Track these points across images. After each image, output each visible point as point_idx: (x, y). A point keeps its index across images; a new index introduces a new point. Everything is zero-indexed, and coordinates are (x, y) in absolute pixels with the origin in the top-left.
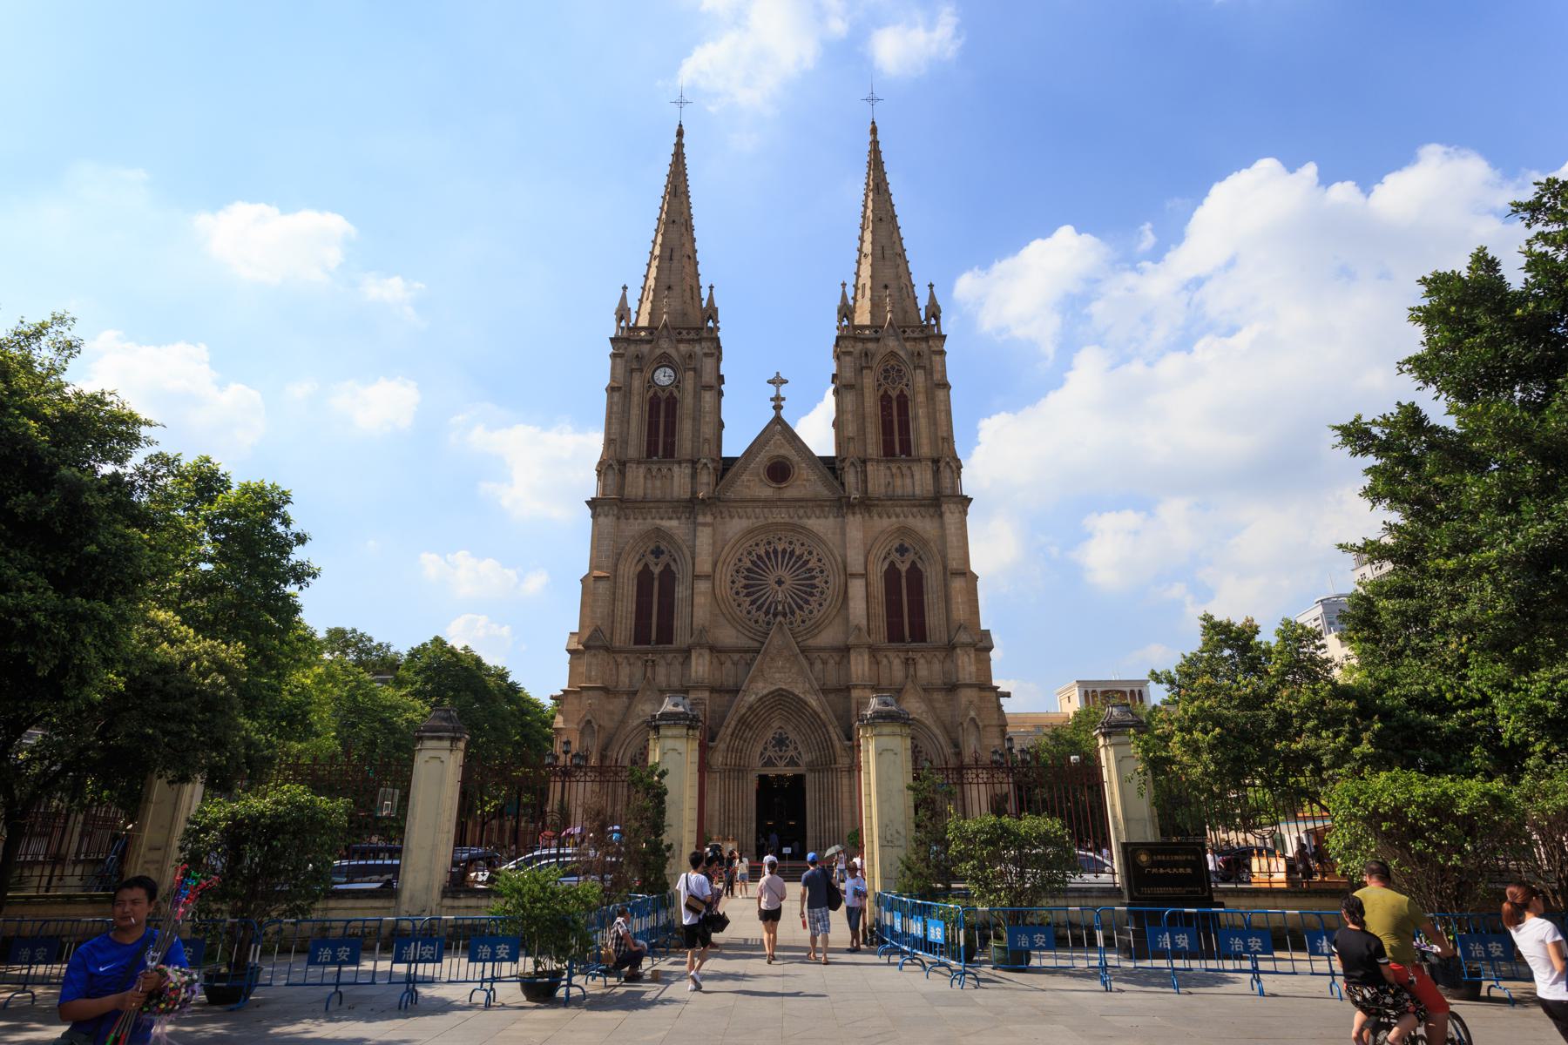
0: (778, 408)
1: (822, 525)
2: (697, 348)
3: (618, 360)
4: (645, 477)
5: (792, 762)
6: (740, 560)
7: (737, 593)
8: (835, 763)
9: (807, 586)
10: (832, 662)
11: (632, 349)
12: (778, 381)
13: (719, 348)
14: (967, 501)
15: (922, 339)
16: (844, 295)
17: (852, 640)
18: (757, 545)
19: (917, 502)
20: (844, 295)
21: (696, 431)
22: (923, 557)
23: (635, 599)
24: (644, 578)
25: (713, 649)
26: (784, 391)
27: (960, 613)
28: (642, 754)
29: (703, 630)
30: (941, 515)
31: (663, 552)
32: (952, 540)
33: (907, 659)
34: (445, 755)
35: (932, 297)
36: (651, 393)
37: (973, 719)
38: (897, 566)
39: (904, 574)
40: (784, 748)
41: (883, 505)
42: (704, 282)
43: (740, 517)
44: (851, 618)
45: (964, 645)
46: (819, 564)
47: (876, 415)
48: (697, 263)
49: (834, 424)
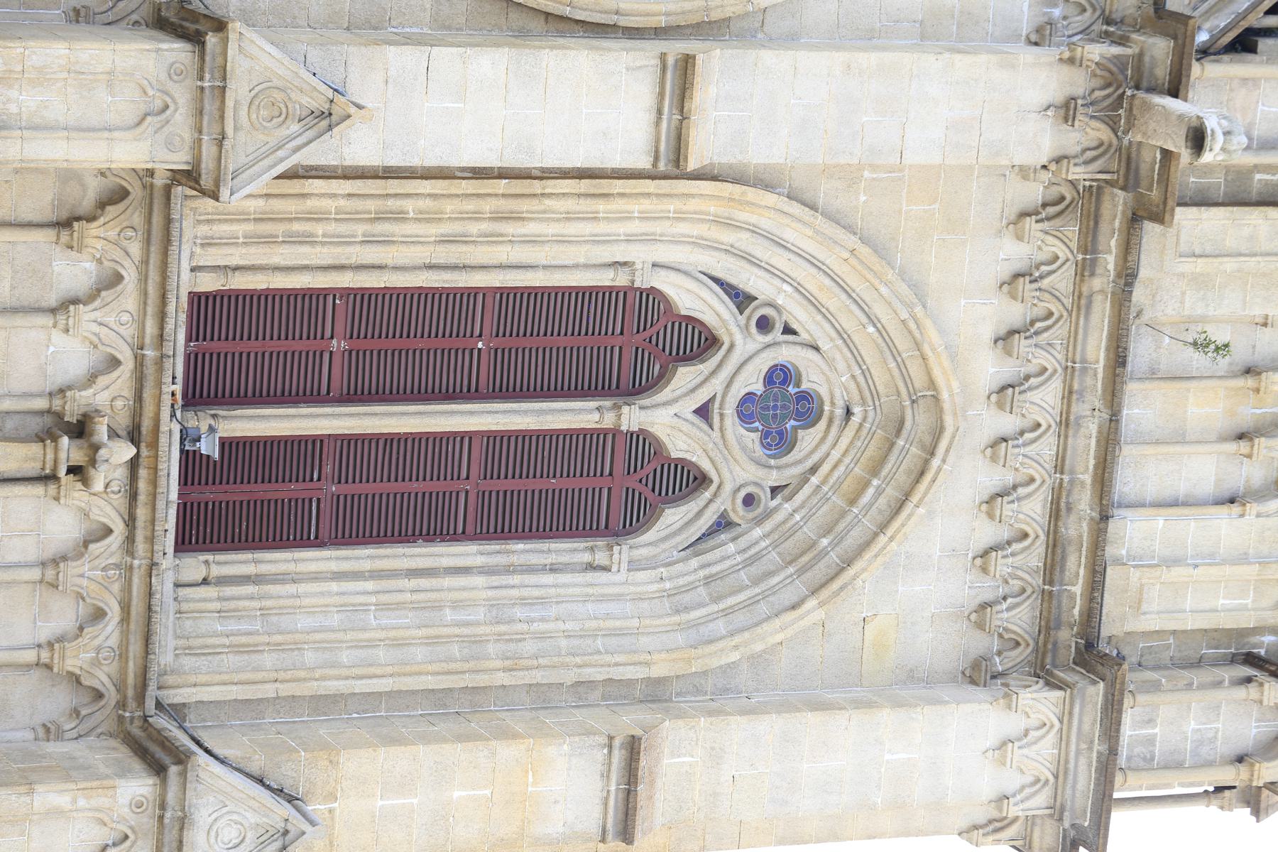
19: (1077, 528)
22: (728, 549)
33: (80, 429)
38: (685, 375)
39: (632, 417)
41: (1081, 303)
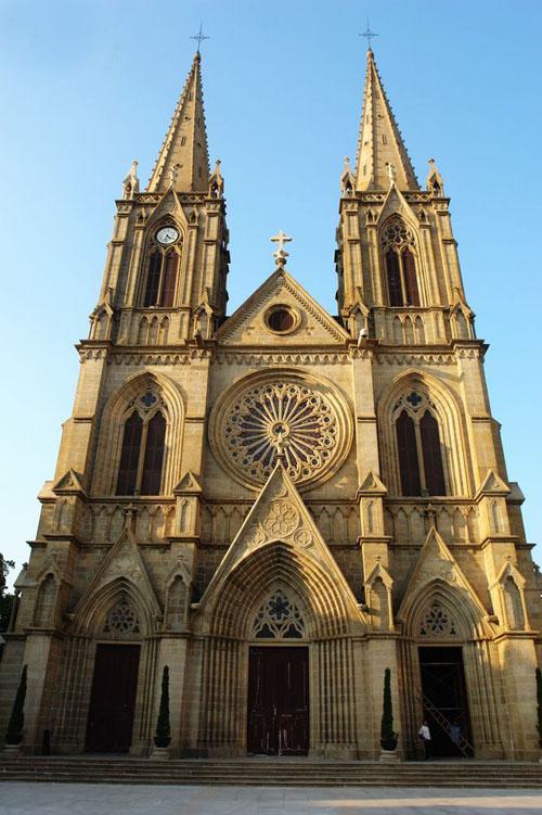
3: (122, 219)
4: (141, 326)
5: (292, 633)
6: (237, 408)
7: (233, 442)
8: (345, 632)
9: (311, 434)
10: (339, 516)
13: (223, 207)
14: (483, 347)
18: (256, 392)
23: (120, 447)
24: (133, 425)
28: (115, 619)
33: (426, 513)
36: (153, 250)
39: (417, 422)
40: (283, 615)
43: (240, 363)
46: (324, 412)
47: (381, 269)
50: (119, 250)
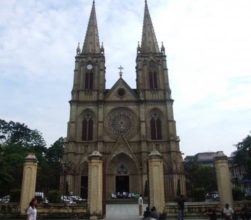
0: (121, 75)
1: (132, 107)
2: (99, 59)
5: (125, 173)
11: (81, 59)
12: (121, 68)
13: (104, 59)
14: (172, 101)
15: (159, 57)
16: (139, 45)
17: (142, 139)
20: (139, 45)
21: (98, 82)
24: (84, 122)
25: (103, 142)
26: (122, 71)
27: (171, 131)
29: (101, 137)
30: (166, 105)
31: (89, 115)
32: (169, 111)
34: (32, 167)
35: (163, 45)
37: (174, 160)
42: (100, 42)
44: (142, 133)
45: (172, 140)
48: (98, 37)
49: (137, 80)
50: (77, 73)
